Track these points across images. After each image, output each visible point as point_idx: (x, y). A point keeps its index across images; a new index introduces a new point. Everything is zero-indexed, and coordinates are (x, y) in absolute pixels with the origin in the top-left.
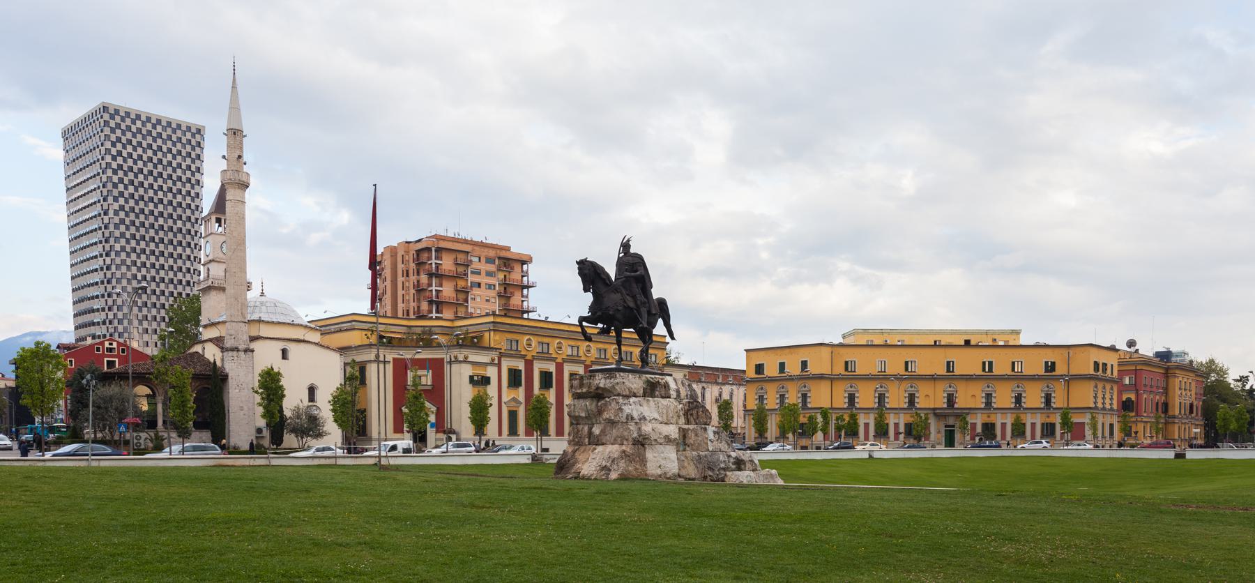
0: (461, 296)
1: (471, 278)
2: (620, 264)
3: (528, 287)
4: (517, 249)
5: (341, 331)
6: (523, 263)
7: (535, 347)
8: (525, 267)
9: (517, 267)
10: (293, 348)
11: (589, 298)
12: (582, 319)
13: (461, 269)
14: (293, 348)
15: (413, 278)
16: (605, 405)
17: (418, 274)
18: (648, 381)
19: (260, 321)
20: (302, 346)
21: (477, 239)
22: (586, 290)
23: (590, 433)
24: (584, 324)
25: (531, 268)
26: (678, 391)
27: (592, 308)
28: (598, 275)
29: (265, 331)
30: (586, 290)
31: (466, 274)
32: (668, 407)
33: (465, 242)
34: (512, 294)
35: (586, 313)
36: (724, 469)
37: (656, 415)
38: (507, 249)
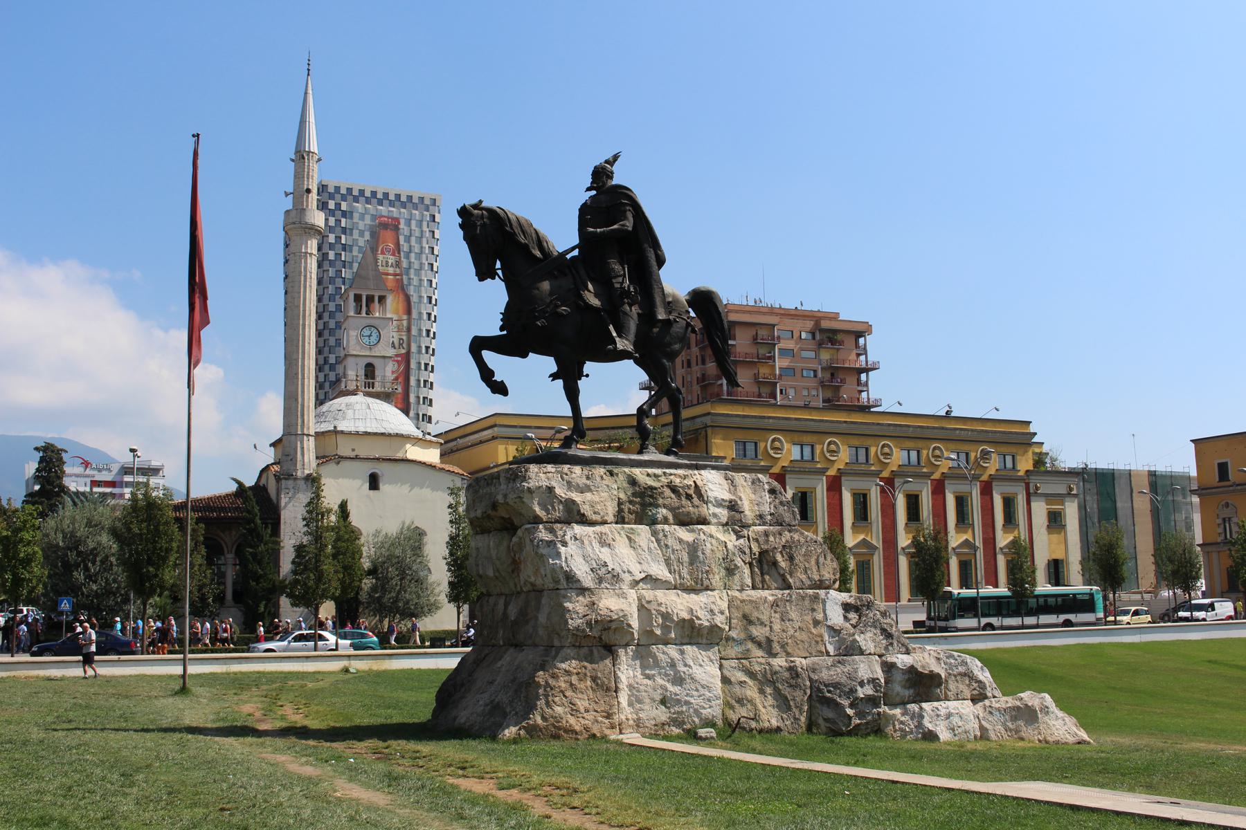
0: (765, 390)
1: (780, 363)
2: (587, 214)
3: (867, 370)
4: (849, 313)
5: (481, 442)
6: (859, 334)
7: (844, 456)
8: (861, 341)
9: (849, 341)
10: (382, 469)
11: (495, 294)
12: (478, 346)
13: (763, 351)
14: (382, 469)
15: (697, 370)
16: (521, 546)
17: (703, 363)
18: (633, 482)
19: (335, 432)
20: (401, 466)
21: (789, 304)
22: (484, 273)
23: (505, 615)
24: (489, 356)
25: (871, 342)
26: (733, 507)
27: (510, 317)
28: (512, 236)
29: (344, 449)
30: (484, 273)
31: (772, 358)
32: (693, 549)
33: (771, 311)
34: (843, 381)
35: (493, 328)
36: (873, 701)
37: (660, 571)
38: (834, 317)
